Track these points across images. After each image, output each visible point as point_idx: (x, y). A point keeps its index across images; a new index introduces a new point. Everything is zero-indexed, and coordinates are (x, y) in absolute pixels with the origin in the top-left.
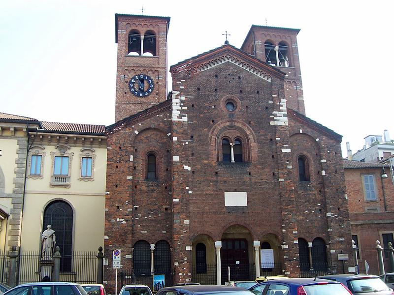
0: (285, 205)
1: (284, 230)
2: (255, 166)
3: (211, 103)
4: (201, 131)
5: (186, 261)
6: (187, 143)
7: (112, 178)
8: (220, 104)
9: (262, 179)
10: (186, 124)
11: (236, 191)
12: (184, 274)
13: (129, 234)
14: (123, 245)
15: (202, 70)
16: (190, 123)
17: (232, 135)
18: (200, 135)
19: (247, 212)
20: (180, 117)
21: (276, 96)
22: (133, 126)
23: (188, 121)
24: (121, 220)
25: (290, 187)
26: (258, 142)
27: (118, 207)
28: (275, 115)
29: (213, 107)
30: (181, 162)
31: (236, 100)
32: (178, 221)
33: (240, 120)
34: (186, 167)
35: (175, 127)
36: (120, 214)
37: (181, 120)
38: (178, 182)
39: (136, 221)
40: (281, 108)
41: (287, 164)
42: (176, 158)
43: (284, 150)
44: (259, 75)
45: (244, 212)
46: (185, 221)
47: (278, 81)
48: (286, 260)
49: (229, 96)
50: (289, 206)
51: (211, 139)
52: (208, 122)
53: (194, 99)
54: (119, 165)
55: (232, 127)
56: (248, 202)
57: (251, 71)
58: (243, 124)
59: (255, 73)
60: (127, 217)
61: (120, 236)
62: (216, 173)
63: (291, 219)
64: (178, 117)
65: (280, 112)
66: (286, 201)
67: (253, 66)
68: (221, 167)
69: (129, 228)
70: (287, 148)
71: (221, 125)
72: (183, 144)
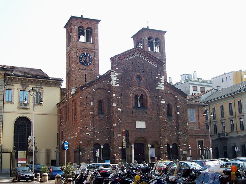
1: (161, 140)
2: (149, 109)
11: (141, 121)
18: (125, 93)
24: (88, 134)
28: (159, 84)
43: (162, 102)
49: (138, 74)
55: (139, 90)
60: (91, 132)
62: (132, 112)
70: (163, 101)
71: (135, 88)
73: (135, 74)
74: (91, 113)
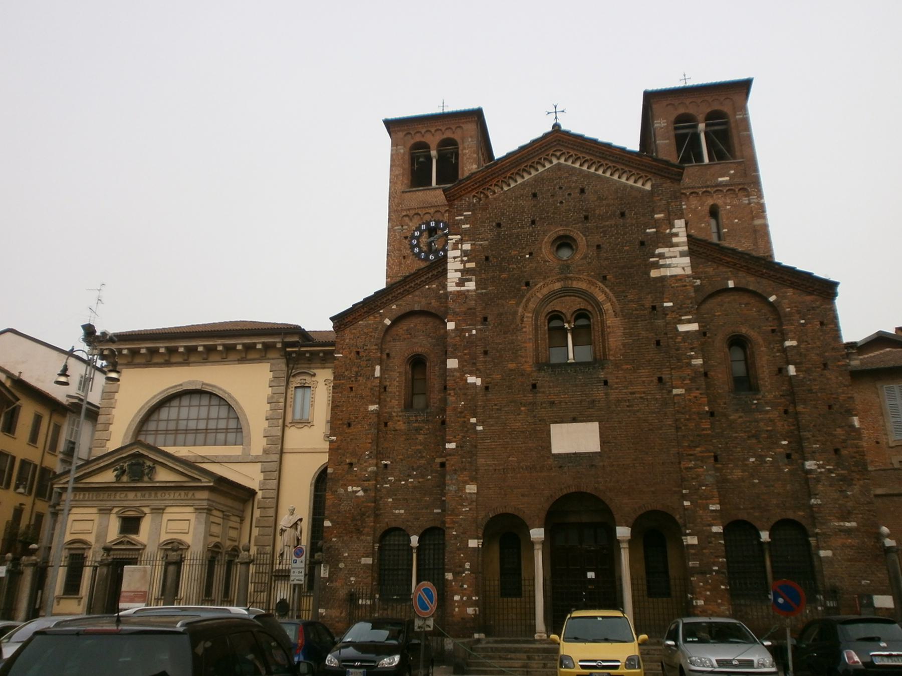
0: (689, 446)
1: (686, 503)
2: (617, 366)
3: (523, 248)
4: (503, 305)
5: (468, 570)
6: (474, 332)
7: (342, 411)
8: (541, 248)
9: (632, 393)
10: (472, 296)
11: (574, 420)
12: (465, 598)
13: (368, 517)
14: (358, 538)
15: (506, 188)
16: (482, 293)
17: (569, 306)
18: (500, 315)
19: (601, 464)
20: (461, 283)
21: (661, 216)
22: (381, 311)
23: (477, 289)
24: (355, 489)
25: (700, 405)
26: (623, 316)
27: (351, 464)
28: (661, 256)
29: (528, 256)
30: (463, 370)
31: (575, 236)
32: (453, 488)
34: (471, 379)
35: (451, 304)
36: (355, 478)
37: (463, 288)
38: (455, 409)
40: (675, 240)
41: (692, 357)
43: (682, 328)
44: (624, 180)
46: (468, 486)
47: (667, 185)
48: (693, 572)
49: (560, 230)
50: (698, 449)
51: (523, 321)
52: (517, 286)
53: (490, 245)
54: (354, 385)
55: (567, 292)
56: (603, 442)
57: (608, 175)
58: (591, 283)
59: (616, 177)
60: (366, 483)
61: (352, 521)
62: (534, 386)
63: (703, 478)
64: (458, 285)
65: (672, 249)
66: (691, 438)
67: (610, 164)
68: (543, 373)
69: (369, 504)
70: (689, 322)
71: (541, 290)
72: (467, 335)
73: (545, 233)
74: (373, 407)
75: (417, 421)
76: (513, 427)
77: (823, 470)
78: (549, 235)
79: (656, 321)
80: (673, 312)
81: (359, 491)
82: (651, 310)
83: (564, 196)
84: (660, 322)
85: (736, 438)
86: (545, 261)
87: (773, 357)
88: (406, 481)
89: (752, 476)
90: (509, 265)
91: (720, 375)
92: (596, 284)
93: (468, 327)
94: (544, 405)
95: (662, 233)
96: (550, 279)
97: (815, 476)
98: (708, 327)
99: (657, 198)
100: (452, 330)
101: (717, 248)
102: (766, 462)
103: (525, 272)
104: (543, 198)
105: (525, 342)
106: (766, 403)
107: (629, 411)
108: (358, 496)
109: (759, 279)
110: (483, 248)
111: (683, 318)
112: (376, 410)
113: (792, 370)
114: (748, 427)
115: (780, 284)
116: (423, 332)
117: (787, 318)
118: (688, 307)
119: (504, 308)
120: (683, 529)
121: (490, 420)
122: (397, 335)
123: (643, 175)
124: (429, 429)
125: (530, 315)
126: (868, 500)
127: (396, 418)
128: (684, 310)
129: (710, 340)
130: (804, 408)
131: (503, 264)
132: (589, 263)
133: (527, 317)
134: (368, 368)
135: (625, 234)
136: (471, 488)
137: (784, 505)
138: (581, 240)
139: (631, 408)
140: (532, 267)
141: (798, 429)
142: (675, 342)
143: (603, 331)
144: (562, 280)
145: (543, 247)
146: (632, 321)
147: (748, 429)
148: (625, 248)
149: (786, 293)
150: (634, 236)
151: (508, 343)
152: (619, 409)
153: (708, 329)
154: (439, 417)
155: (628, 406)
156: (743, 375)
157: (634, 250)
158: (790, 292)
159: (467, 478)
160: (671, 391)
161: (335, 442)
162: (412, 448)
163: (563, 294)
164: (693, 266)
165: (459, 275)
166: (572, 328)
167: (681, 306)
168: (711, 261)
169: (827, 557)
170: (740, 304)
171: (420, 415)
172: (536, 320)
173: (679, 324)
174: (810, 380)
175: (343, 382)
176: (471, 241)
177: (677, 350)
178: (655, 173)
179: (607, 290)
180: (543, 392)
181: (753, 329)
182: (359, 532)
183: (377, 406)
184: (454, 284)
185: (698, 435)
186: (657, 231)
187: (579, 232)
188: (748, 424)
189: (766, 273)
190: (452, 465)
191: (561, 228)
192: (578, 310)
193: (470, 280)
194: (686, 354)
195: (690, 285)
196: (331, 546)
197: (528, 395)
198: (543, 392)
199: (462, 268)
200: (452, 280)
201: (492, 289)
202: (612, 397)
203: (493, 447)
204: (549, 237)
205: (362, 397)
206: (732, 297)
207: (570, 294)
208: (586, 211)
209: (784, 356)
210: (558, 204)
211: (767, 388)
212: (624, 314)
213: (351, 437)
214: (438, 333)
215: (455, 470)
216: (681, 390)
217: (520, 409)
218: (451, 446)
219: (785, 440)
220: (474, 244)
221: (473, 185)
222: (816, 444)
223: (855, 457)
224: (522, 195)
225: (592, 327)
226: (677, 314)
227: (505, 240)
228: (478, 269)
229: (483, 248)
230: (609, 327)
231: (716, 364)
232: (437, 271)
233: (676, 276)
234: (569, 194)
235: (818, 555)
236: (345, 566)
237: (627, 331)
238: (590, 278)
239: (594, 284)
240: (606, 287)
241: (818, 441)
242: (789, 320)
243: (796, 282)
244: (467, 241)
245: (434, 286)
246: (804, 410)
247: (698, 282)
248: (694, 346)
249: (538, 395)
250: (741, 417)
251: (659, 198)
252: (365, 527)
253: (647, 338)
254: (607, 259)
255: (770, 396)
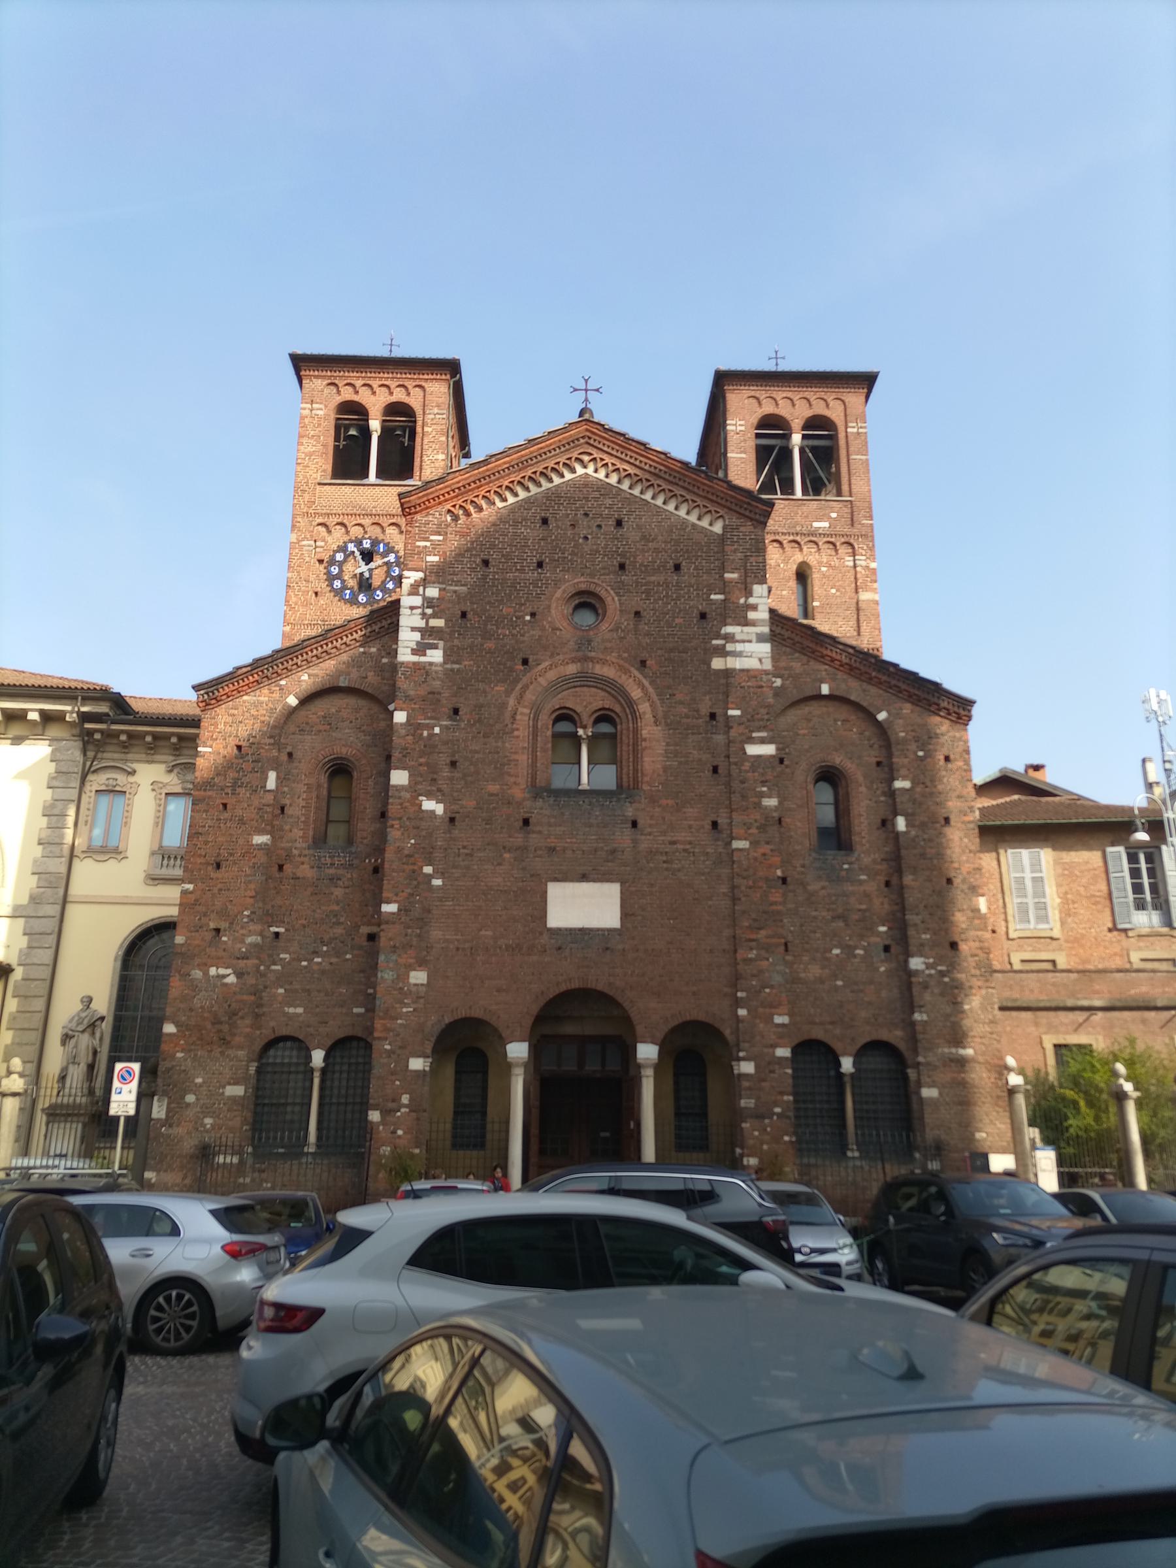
0: (749, 927)
1: (742, 1012)
4: (485, 692)
6: (437, 730)
7: (206, 843)
8: (549, 607)
10: (436, 672)
11: (584, 878)
13: (242, 1018)
14: (222, 1053)
16: (452, 670)
17: (587, 702)
19: (620, 947)
20: (420, 649)
21: (735, 576)
22: (283, 682)
23: (445, 662)
24: (222, 971)
25: (770, 866)
26: (667, 725)
27: (218, 931)
28: (730, 638)
29: (528, 618)
30: (414, 791)
31: (603, 594)
33: (613, 657)
34: (429, 805)
35: (402, 683)
36: (221, 953)
37: (423, 659)
39: (272, 977)
40: (752, 615)
41: (762, 795)
42: (399, 777)
43: (753, 750)
44: (682, 513)
45: (607, 949)
46: (413, 974)
47: (747, 528)
50: (763, 933)
52: (509, 664)
53: (469, 593)
54: (231, 801)
55: (585, 680)
56: (625, 915)
57: (659, 502)
58: (621, 669)
59: (671, 507)
60: (242, 963)
61: (213, 1024)
62: (526, 822)
63: (767, 975)
64: (415, 652)
65: (746, 629)
66: (754, 916)
67: (664, 486)
68: (540, 803)
69: (245, 997)
70: (762, 741)
71: (547, 673)
72: (425, 733)
73: (557, 583)
74: (260, 839)
75: (332, 864)
76: (490, 884)
77: (933, 972)
78: (563, 587)
79: (714, 736)
80: (740, 724)
81: (229, 975)
82: (708, 719)
83: (589, 527)
84: (720, 738)
85: (815, 918)
86: (555, 629)
87: (876, 802)
88: (310, 961)
89: (835, 977)
90: (498, 628)
91: (799, 824)
92: (630, 672)
93: (427, 721)
94: (539, 852)
95: (733, 603)
96: (561, 657)
97: (921, 980)
98: (787, 750)
99: (730, 547)
100: (401, 724)
101: (809, 632)
102: (855, 956)
103: (523, 642)
104: (558, 527)
105: (516, 753)
106: (861, 869)
107: (667, 869)
108: (226, 985)
109: (865, 685)
110: (458, 596)
111: (754, 735)
112: (266, 844)
113: (901, 823)
114: (833, 903)
115: (894, 695)
116: (351, 722)
117: (900, 747)
118: (762, 720)
119: (486, 696)
120: (734, 1050)
121: (454, 871)
122: (307, 723)
123: (712, 509)
124: (351, 879)
125: (527, 711)
126: (990, 1017)
127: (298, 859)
128: (757, 724)
129: (788, 770)
130: (913, 880)
131: (489, 627)
132: (621, 639)
133: (522, 714)
134: (256, 774)
135: (678, 598)
136: (419, 977)
137: (876, 1020)
138: (612, 601)
139: (669, 866)
140: (533, 635)
141: (903, 910)
142: (740, 770)
143: (635, 744)
144: (579, 661)
145: (554, 605)
146: (680, 733)
147: (834, 906)
148: (677, 621)
149: (901, 709)
150: (692, 603)
151: (490, 753)
152: (651, 865)
153: (786, 754)
154: (370, 861)
155: (664, 862)
156: (831, 826)
157: (690, 625)
158: (907, 708)
159: (412, 961)
160: (730, 843)
161: (191, 893)
162: (323, 908)
163: (579, 683)
164: (775, 658)
165: (417, 636)
166: (588, 736)
167: (752, 716)
168: (799, 652)
169: (931, 1099)
170: (836, 720)
171: (339, 856)
172: (536, 719)
173: (747, 743)
174: (924, 840)
175: (209, 793)
176: (439, 583)
177: (743, 782)
178: (730, 509)
179: (646, 683)
180: (540, 832)
181: (851, 758)
182: (224, 1042)
183: (269, 836)
184: (409, 651)
185: (765, 912)
186: (725, 600)
187: (609, 588)
188: (834, 898)
189: (876, 677)
190: (390, 939)
191: (582, 579)
192: (600, 710)
193: (435, 647)
194: (754, 790)
195: (768, 687)
196: (173, 1067)
197: (516, 835)
198: (540, 832)
199: (424, 625)
200: (405, 644)
201: (470, 666)
202: (643, 846)
203: (457, 912)
204: (564, 591)
205: (242, 821)
206: (825, 709)
207: (589, 683)
208: (623, 555)
209: (890, 802)
210: (581, 541)
211: (864, 848)
212: (669, 721)
213: (220, 886)
214: (375, 725)
215: (395, 947)
216: (744, 842)
217: (501, 856)
218: (389, 908)
219: (884, 925)
220: (444, 589)
221: (448, 493)
222: (925, 933)
223: (976, 955)
224: (525, 519)
225: (619, 737)
226: (747, 728)
227: (495, 589)
228: (447, 630)
229: (458, 596)
230: (645, 740)
231: (794, 806)
232: (379, 625)
233: (748, 671)
234: (599, 526)
235: (918, 1093)
236: (197, 1099)
237: (672, 748)
238: (622, 662)
239: (626, 671)
240: (645, 677)
241: (928, 929)
242: (903, 750)
243: (915, 695)
244: (434, 583)
245: (373, 650)
246: (913, 883)
247: (778, 682)
248: (768, 778)
249: (531, 835)
250: (823, 888)
251: (733, 548)
252: (235, 1035)
253: (700, 760)
254: (648, 634)
255: (866, 860)
